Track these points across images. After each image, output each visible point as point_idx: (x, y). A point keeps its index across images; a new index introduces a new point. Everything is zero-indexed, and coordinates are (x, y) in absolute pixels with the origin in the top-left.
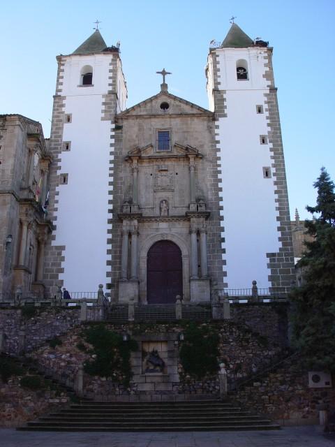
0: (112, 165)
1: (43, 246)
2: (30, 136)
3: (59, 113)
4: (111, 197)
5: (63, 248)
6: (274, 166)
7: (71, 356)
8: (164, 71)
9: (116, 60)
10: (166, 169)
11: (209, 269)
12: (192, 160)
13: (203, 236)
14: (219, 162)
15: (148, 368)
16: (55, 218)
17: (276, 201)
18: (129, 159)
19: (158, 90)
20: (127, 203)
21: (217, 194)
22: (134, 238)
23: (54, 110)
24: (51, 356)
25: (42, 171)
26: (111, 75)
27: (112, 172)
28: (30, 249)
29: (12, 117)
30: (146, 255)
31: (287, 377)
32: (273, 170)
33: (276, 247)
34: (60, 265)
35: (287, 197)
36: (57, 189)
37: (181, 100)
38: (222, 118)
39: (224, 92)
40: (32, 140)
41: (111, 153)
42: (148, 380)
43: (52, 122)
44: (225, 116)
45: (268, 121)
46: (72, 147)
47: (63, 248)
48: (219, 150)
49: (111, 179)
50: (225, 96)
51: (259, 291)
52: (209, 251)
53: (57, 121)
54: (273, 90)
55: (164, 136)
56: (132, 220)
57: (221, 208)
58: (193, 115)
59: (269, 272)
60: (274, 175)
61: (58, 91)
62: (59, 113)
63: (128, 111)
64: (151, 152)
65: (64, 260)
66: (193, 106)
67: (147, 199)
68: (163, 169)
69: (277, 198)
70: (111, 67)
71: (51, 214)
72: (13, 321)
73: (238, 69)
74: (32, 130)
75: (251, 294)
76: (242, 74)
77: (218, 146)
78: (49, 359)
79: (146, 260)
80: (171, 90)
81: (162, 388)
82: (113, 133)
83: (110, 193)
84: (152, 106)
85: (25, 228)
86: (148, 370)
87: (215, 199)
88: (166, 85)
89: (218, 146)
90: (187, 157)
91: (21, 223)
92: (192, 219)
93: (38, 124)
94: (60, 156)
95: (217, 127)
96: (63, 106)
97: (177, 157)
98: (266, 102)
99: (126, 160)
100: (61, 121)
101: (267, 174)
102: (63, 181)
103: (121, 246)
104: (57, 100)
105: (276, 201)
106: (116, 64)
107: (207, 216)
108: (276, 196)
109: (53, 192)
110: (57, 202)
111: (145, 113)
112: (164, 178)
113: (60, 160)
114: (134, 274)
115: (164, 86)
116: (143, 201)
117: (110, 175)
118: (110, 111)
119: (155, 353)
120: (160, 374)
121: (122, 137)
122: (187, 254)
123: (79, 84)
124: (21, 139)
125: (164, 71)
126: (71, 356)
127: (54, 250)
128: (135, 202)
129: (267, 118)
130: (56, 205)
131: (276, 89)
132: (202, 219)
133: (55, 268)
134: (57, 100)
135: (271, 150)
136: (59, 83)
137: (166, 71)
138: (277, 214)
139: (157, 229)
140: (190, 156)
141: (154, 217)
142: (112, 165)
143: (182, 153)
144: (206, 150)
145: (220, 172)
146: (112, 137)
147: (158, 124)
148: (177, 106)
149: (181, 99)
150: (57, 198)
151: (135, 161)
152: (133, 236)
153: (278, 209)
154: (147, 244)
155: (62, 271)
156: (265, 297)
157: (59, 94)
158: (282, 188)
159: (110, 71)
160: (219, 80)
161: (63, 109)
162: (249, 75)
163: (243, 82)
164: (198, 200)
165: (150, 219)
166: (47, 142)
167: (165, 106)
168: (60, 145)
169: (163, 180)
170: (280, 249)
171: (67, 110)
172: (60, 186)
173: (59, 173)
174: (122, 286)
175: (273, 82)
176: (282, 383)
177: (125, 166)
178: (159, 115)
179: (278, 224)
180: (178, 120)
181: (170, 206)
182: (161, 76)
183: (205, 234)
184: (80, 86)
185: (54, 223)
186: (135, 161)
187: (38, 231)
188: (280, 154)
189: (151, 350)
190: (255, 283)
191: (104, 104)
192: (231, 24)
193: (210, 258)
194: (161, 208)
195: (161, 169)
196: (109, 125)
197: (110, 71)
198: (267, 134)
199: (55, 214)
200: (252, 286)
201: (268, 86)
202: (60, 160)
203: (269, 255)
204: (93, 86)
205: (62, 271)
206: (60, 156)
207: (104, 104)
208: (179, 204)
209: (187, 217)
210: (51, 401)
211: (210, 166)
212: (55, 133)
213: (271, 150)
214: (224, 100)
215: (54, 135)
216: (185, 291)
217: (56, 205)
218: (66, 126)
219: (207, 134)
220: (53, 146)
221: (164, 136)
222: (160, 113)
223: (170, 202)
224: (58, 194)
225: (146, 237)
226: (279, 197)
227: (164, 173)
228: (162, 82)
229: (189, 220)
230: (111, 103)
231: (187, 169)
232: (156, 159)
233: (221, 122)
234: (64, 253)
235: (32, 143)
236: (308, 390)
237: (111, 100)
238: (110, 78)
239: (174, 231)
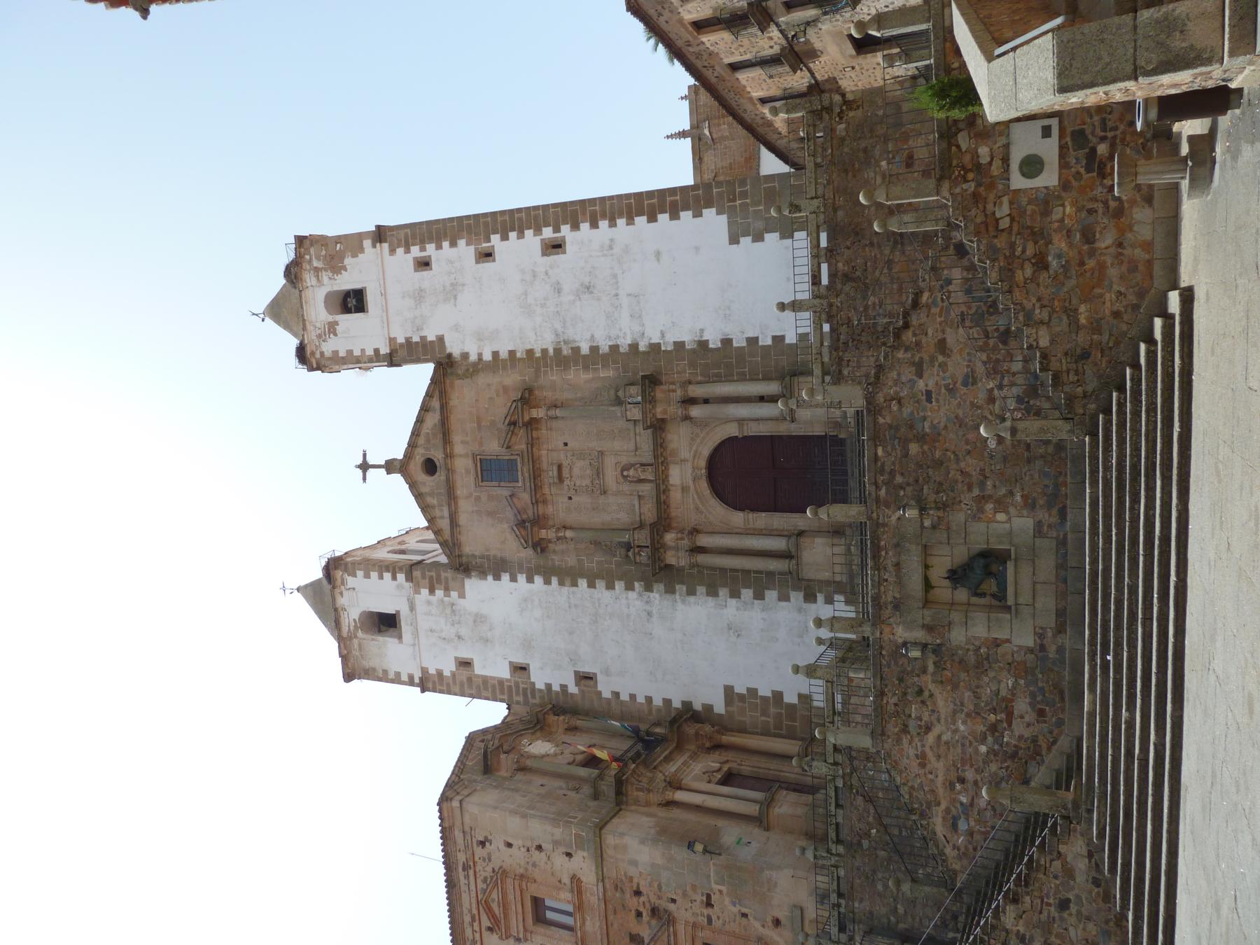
0: (554, 580)
1: (726, 739)
2: (488, 768)
3: (455, 683)
4: (619, 585)
5: (729, 690)
6: (538, 231)
7: (962, 780)
8: (360, 467)
9: (346, 564)
10: (555, 468)
11: (767, 378)
12: (535, 413)
13: (697, 391)
14: (538, 355)
15: (993, 596)
16: (667, 702)
17: (613, 224)
18: (540, 547)
19: (398, 478)
20: (630, 554)
21: (605, 355)
22: (704, 541)
23: (449, 693)
24: (963, 826)
25: (572, 729)
26: (374, 575)
27: (568, 581)
28: (729, 779)
29: (445, 814)
30: (741, 514)
31: (1024, 251)
32: (548, 232)
33: (714, 222)
34: (764, 699)
35: (603, 199)
36: (607, 694)
37: (415, 433)
38: (447, 344)
39: (392, 340)
40: (499, 762)
41: (530, 580)
42: (1025, 598)
43: (473, 697)
44: (441, 339)
45: (446, 244)
46: (520, 659)
47: (729, 690)
48: (512, 353)
49: (583, 583)
50: (401, 340)
51: (800, 297)
52: (728, 378)
53: (470, 686)
54: (380, 234)
55: (489, 470)
56: (664, 546)
57: (634, 347)
58: (442, 407)
59: (772, 238)
60: (557, 230)
61: (411, 682)
62: (455, 683)
63: (443, 544)
64: (525, 497)
65: (756, 690)
66: (425, 408)
67: (621, 507)
68: (555, 473)
69: (606, 222)
70: (360, 573)
71: (659, 710)
72: (880, 875)
73: (346, 310)
74: (484, 758)
75: (807, 315)
76: (353, 302)
77: (504, 354)
78: (971, 833)
79: (751, 515)
80: (400, 455)
81: (1046, 565)
82: (490, 578)
83: (610, 586)
84: (432, 494)
85: (680, 796)
86: (1001, 596)
87: (615, 362)
88: (387, 462)
89: (504, 354)
90: (532, 424)
91: (670, 804)
92: (659, 416)
93: (471, 739)
94: (540, 685)
95: (465, 356)
96: (440, 674)
97: (532, 443)
98: (408, 251)
99: (543, 550)
100: (470, 679)
101: (556, 247)
102: (592, 683)
103: (723, 570)
104: (430, 685)
105: (613, 224)
106: (353, 563)
107: (651, 381)
108: (603, 224)
109: (613, 704)
110: (633, 697)
111: (446, 514)
112: (576, 471)
113: (549, 686)
114: (778, 544)
115: (390, 466)
116: (624, 518)
117: (575, 584)
118: (446, 579)
119: (956, 576)
120: (1010, 566)
121: (495, 556)
122: (735, 425)
123: (396, 640)
124: (491, 796)
125: (360, 467)
126: (962, 780)
127: (734, 709)
128: (626, 538)
129: (439, 247)
130: (641, 699)
131: (378, 227)
132: (659, 393)
133: (772, 710)
134: (430, 685)
135: (505, 238)
136: (397, 680)
137: (360, 461)
138: (641, 221)
139: (684, 489)
140: (527, 418)
141: (658, 496)
142: (554, 580)
143: (522, 432)
144: (512, 379)
145: (558, 351)
146: (497, 577)
147: (465, 480)
148: (428, 441)
149: (413, 433)
150: (624, 697)
151: (543, 533)
152: (699, 544)
153: (630, 221)
154: (717, 511)
155: (778, 696)
156: (816, 279)
157: (417, 681)
158: (584, 214)
159: (367, 576)
160: (370, 352)
161: (447, 673)
162: (357, 286)
163: (371, 299)
164: (619, 402)
165: (662, 504)
166: (519, 709)
167: (430, 467)
168: (517, 684)
169: (580, 472)
170: (718, 214)
171: (449, 668)
172: (599, 689)
173: (573, 689)
174: (808, 573)
175: (360, 236)
176: (1041, 263)
177: (554, 551)
178: (448, 480)
179: (663, 218)
180: (457, 438)
181: (633, 460)
182: (371, 472)
183: (691, 388)
184: (400, 637)
185: (677, 704)
186: (543, 533)
187: (693, 747)
188: (512, 221)
189: (947, 583)
190: (782, 307)
191: (432, 591)
192: (267, 319)
193: (744, 374)
194: (641, 481)
195: (556, 480)
196: (475, 587)
197: (367, 576)
198: (472, 248)
199: (658, 702)
200: (789, 314)
201: (374, 246)
202: (549, 686)
203: (734, 240)
204: (398, 612)
205: (778, 696)
206: (540, 685)
207: (432, 591)
208: (624, 444)
209: (658, 427)
210: (1080, 878)
211: (546, 372)
212: (494, 692)
213: (505, 238)
214: (408, 340)
215: (499, 697)
216: (818, 431)
217: (641, 699)
218: (479, 669)
219: (482, 379)
220: (520, 699)
221: (489, 470)
222: (443, 478)
223: (624, 460)
224: (617, 695)
225: (702, 512)
226: (604, 217)
227: (565, 473)
228: (383, 471)
229: (663, 420)
230: (431, 577)
231: (554, 424)
232: (536, 487)
233: (454, 347)
234: (740, 689)
235: (506, 762)
236: (1065, 185)
237: (424, 577)
238: (381, 577)
239: (685, 453)
